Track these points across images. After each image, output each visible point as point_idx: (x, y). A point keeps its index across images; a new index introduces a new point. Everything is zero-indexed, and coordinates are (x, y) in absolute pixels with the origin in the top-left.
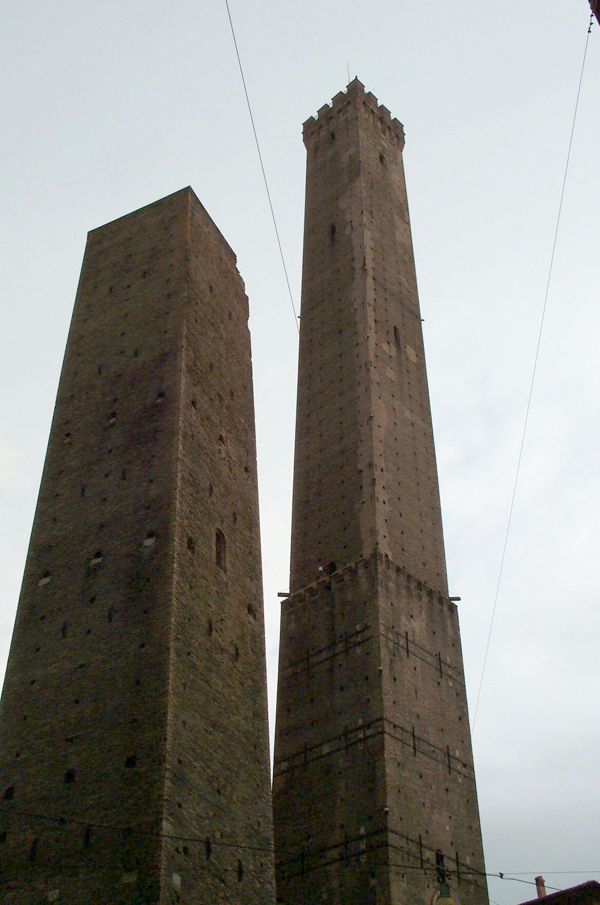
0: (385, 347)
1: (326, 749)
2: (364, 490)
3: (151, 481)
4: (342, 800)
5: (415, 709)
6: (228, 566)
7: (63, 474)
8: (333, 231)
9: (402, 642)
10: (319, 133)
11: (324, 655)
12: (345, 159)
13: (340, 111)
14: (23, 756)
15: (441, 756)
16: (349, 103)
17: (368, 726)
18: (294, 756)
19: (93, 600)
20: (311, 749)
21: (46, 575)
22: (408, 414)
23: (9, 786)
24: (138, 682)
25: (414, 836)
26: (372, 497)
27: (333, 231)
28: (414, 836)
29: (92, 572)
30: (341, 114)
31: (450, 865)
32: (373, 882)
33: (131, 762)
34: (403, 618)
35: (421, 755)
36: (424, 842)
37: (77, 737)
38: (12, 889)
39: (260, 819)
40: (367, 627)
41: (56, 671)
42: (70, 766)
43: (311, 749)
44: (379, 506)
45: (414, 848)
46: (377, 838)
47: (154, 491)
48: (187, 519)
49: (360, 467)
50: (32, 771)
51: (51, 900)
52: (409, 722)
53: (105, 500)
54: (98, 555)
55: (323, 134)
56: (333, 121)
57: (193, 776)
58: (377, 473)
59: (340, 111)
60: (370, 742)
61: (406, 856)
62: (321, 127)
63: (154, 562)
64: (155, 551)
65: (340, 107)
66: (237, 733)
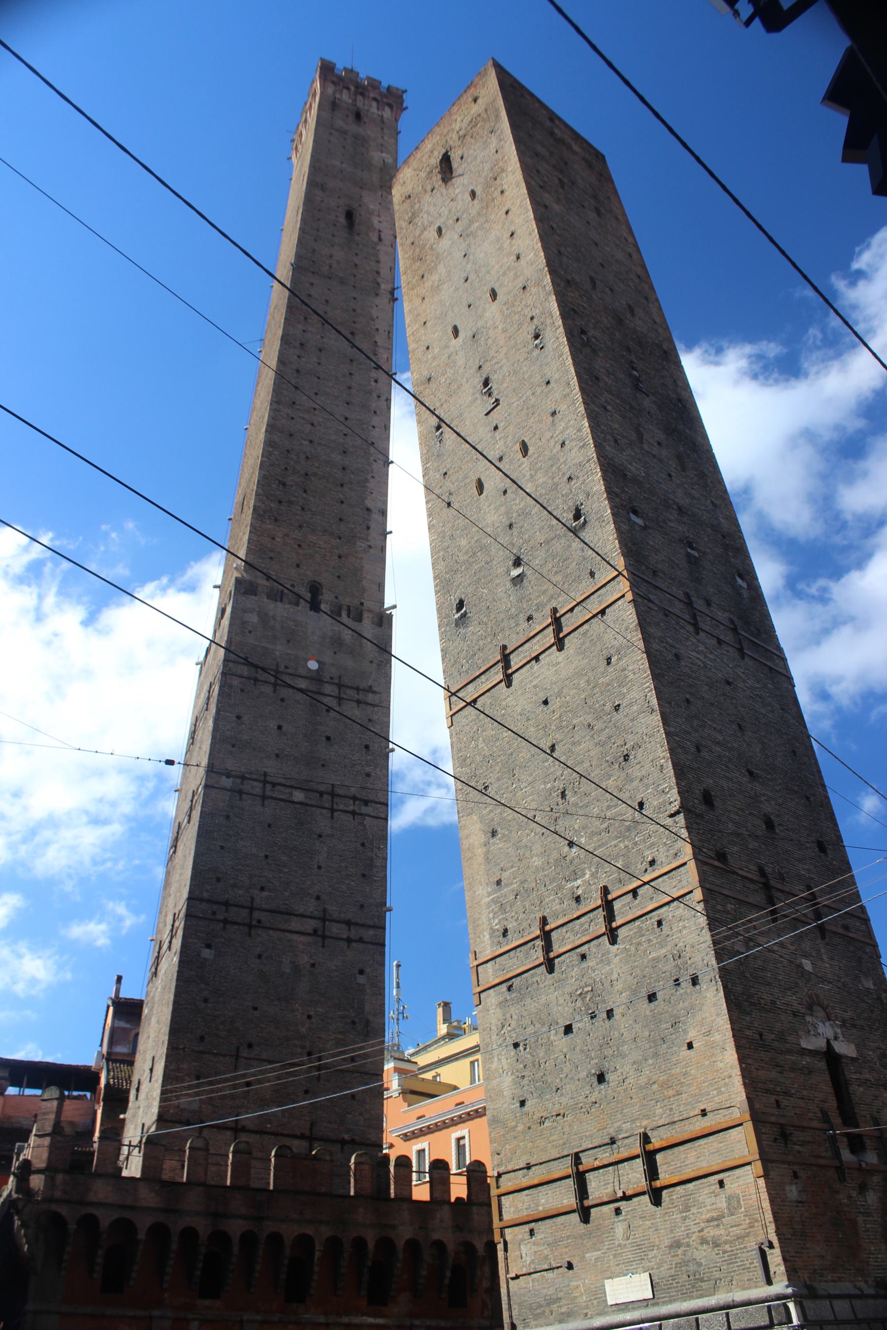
1: (298, 796)
4: (319, 867)
8: (349, 215)
13: (375, 99)
14: (704, 754)
17: (366, 803)
18: (243, 778)
23: (704, 786)
27: (349, 215)
30: (374, 104)
32: (361, 979)
40: (370, 690)
46: (371, 932)
49: (369, 503)
56: (360, 98)
60: (368, 821)
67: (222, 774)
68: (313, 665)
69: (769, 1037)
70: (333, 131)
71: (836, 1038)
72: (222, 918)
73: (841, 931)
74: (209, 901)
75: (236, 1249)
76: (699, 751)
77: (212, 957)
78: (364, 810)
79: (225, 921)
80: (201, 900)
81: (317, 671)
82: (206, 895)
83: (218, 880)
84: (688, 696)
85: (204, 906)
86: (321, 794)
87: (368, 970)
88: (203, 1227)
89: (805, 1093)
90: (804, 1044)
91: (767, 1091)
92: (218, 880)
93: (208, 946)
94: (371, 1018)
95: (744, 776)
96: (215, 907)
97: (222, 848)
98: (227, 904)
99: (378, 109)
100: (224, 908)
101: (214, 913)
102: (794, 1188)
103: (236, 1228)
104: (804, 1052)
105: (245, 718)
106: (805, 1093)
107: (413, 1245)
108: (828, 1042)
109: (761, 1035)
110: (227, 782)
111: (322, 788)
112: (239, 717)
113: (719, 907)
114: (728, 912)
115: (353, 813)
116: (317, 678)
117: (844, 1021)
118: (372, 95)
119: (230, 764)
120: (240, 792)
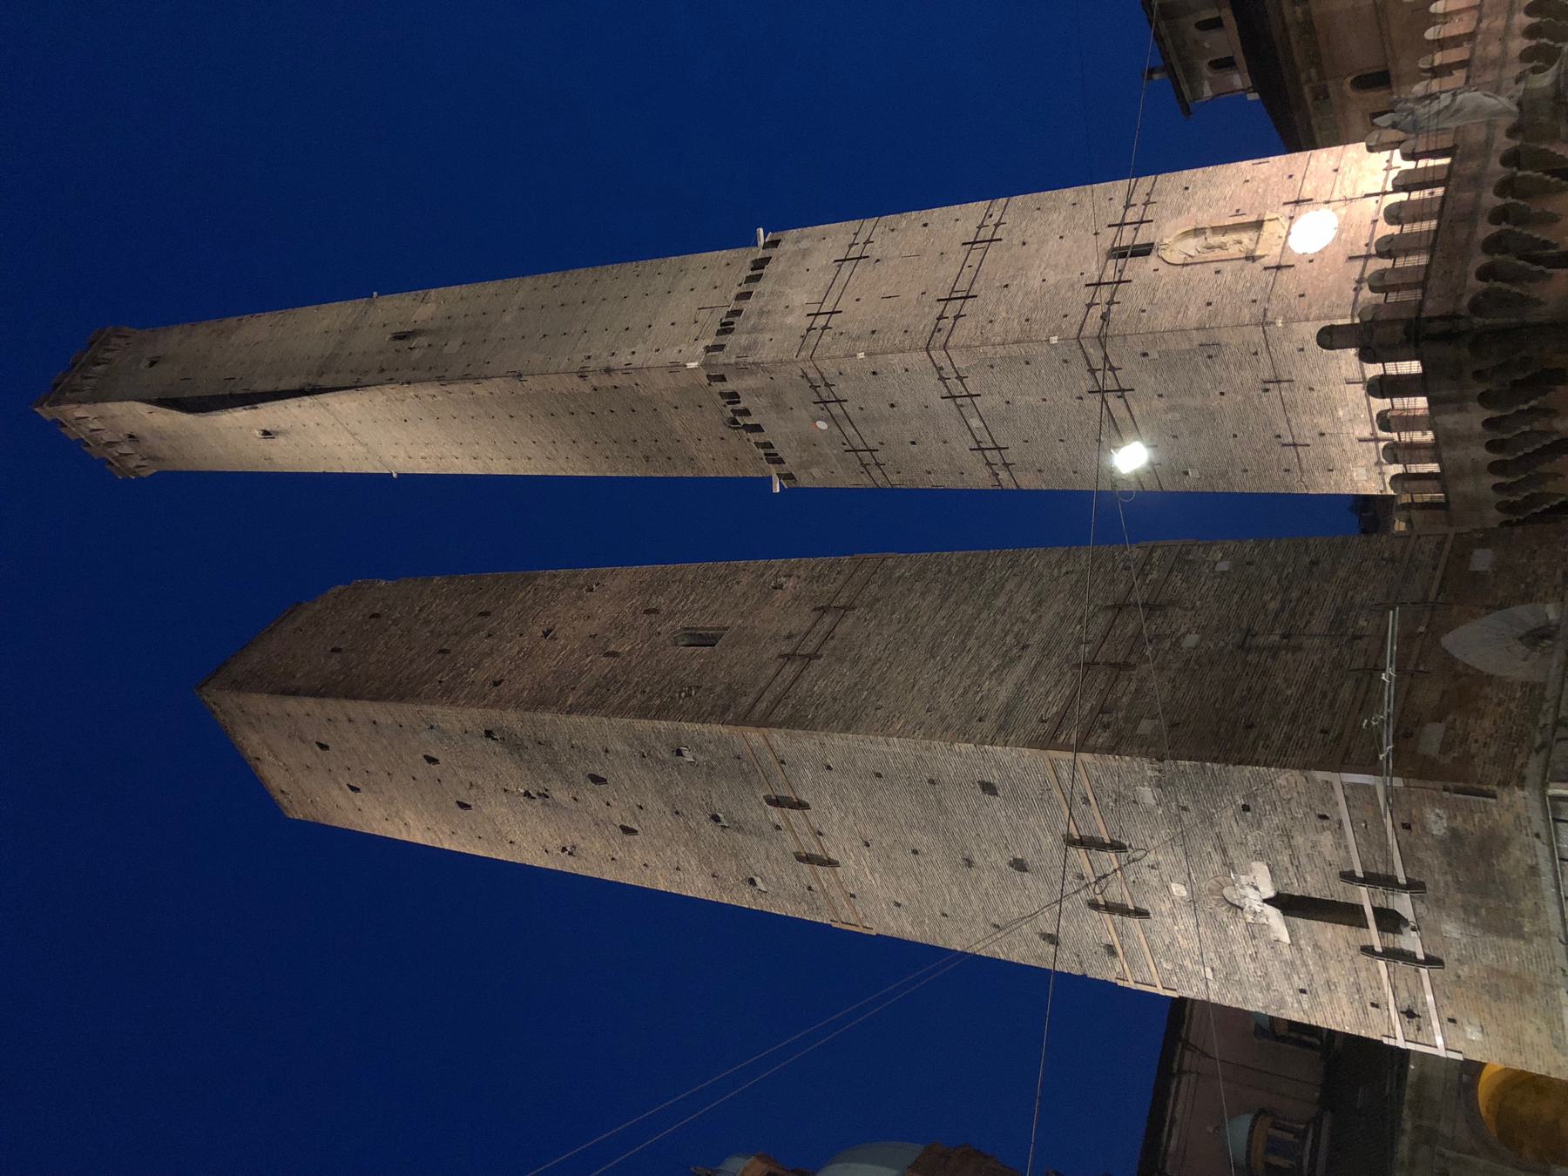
0: (416, 354)
1: (975, 423)
2: (617, 382)
5: (915, 295)
6: (715, 623)
9: (821, 321)
11: (850, 431)
15: (975, 255)
19: (778, 828)
20: (979, 443)
21: (752, 882)
22: (507, 318)
23: (1037, 938)
24: (879, 775)
25: (1085, 295)
26: (628, 370)
28: (1085, 295)
31: (1127, 237)
33: (989, 788)
34: (789, 320)
35: (976, 285)
36: (1096, 280)
38: (1174, 939)
39: (1064, 570)
40: (804, 375)
42: (1003, 864)
43: (979, 443)
44: (637, 361)
45: (1105, 293)
48: (650, 699)
52: (931, 307)
57: (1004, 694)
58: (592, 364)
61: (1114, 308)
63: (711, 747)
64: (699, 748)
66: (943, 613)
68: (822, 425)
78: (948, 369)
81: (825, 420)
86: (959, 407)
87: (1140, 350)
90: (1286, 938)
94: (1196, 343)
102: (1469, 1029)
105: (927, 468)
107: (1491, 446)
108: (1265, 901)
111: (953, 405)
115: (960, 378)
116: (833, 419)
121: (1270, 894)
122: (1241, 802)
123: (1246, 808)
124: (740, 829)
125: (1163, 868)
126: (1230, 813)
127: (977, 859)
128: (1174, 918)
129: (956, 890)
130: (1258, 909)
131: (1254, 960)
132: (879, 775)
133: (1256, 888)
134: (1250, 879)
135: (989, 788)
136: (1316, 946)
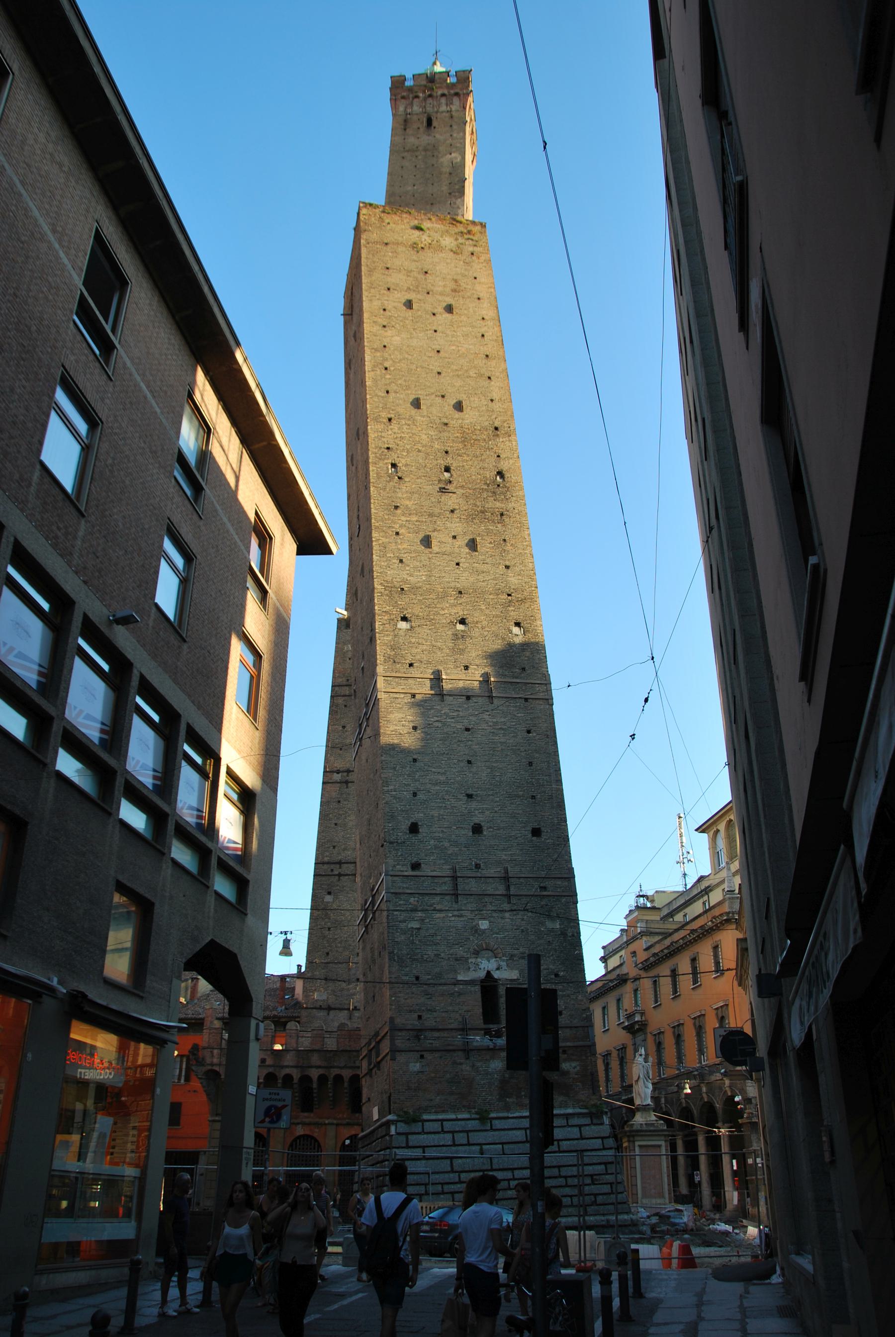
3: (507, 567)
7: (399, 511)
10: (412, 104)
12: (445, 160)
13: (443, 95)
14: (421, 796)
16: (457, 94)
19: (466, 668)
23: (413, 820)
24: (530, 764)
29: (456, 636)
30: (443, 100)
37: (477, 795)
38: (440, 911)
41: (440, 725)
47: (514, 580)
50: (435, 813)
51: (482, 927)
53: (458, 564)
54: (463, 622)
55: (416, 108)
56: (430, 100)
59: (443, 95)
62: (417, 97)
65: (446, 92)
67: (333, 772)
69: (424, 978)
70: (405, 154)
71: (498, 969)
72: (337, 873)
73: (538, 892)
74: (328, 863)
75: (346, 1085)
76: (415, 794)
77: (331, 900)
79: (340, 875)
80: (323, 863)
82: (326, 859)
83: (334, 847)
84: (415, 757)
85: (326, 867)
88: (296, 1074)
89: (451, 1008)
90: (460, 978)
91: (410, 1011)
92: (334, 847)
93: (329, 893)
95: (461, 800)
96: (332, 866)
97: (336, 824)
98: (340, 863)
99: (447, 105)
100: (338, 866)
101: (332, 870)
102: (418, 1064)
103: (314, 1074)
104: (457, 983)
106: (451, 1008)
108: (489, 973)
109: (417, 978)
110: (337, 777)
112: (344, 727)
113: (402, 902)
114: (410, 904)
117: (512, 957)
118: (440, 92)
119: (339, 764)
120: (347, 782)
121: (496, 975)
122: (562, 974)
123: (557, 975)
124: (456, 636)
125: (500, 920)
126: (551, 966)
127: (474, 805)
128: (458, 916)
129: (443, 778)
130: (482, 966)
131: (435, 955)
132: (530, 764)
133: (498, 969)
134: (505, 967)
135: (536, 832)
136: (460, 994)
